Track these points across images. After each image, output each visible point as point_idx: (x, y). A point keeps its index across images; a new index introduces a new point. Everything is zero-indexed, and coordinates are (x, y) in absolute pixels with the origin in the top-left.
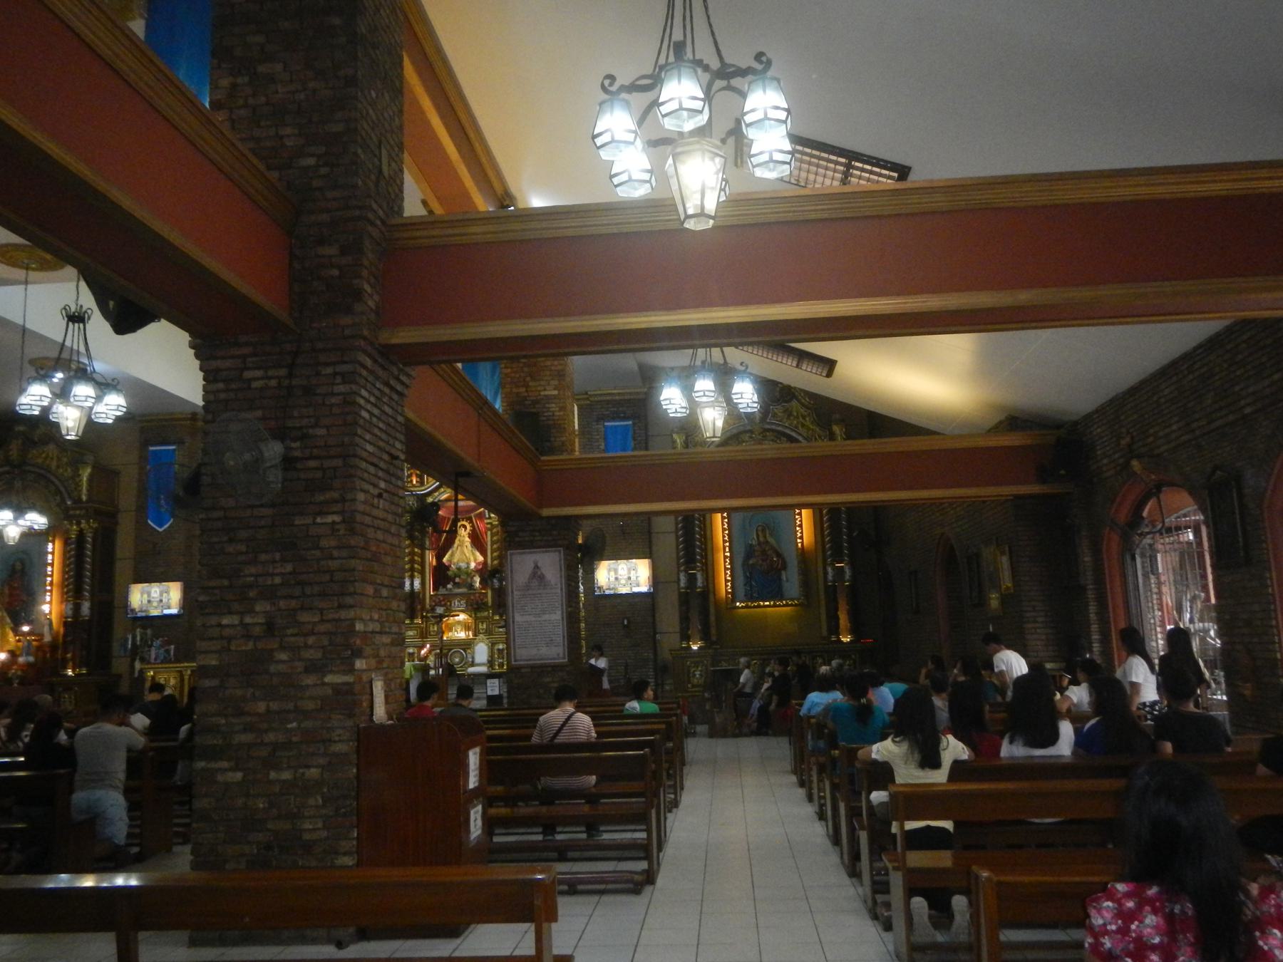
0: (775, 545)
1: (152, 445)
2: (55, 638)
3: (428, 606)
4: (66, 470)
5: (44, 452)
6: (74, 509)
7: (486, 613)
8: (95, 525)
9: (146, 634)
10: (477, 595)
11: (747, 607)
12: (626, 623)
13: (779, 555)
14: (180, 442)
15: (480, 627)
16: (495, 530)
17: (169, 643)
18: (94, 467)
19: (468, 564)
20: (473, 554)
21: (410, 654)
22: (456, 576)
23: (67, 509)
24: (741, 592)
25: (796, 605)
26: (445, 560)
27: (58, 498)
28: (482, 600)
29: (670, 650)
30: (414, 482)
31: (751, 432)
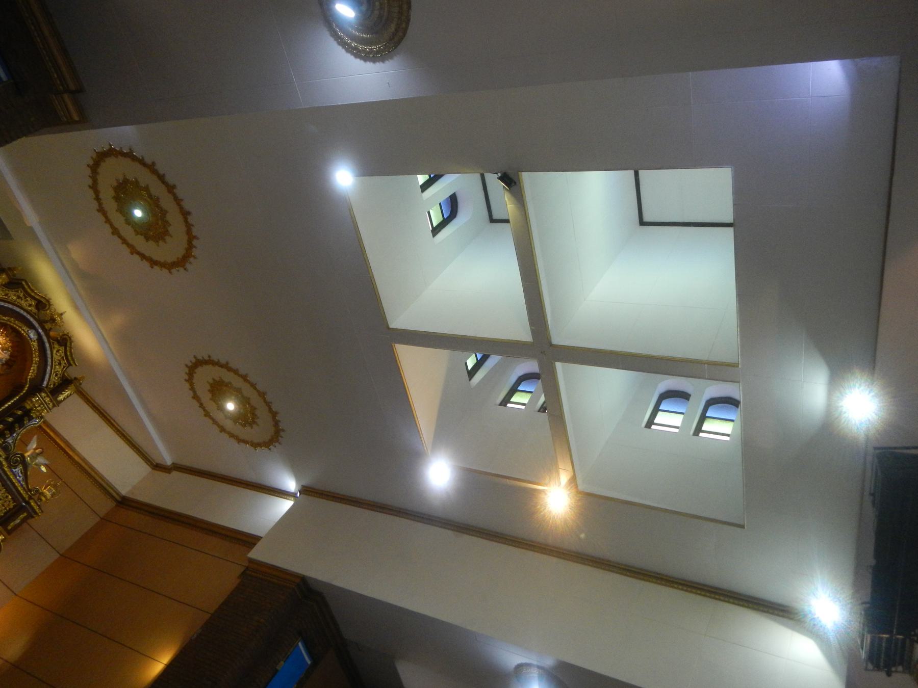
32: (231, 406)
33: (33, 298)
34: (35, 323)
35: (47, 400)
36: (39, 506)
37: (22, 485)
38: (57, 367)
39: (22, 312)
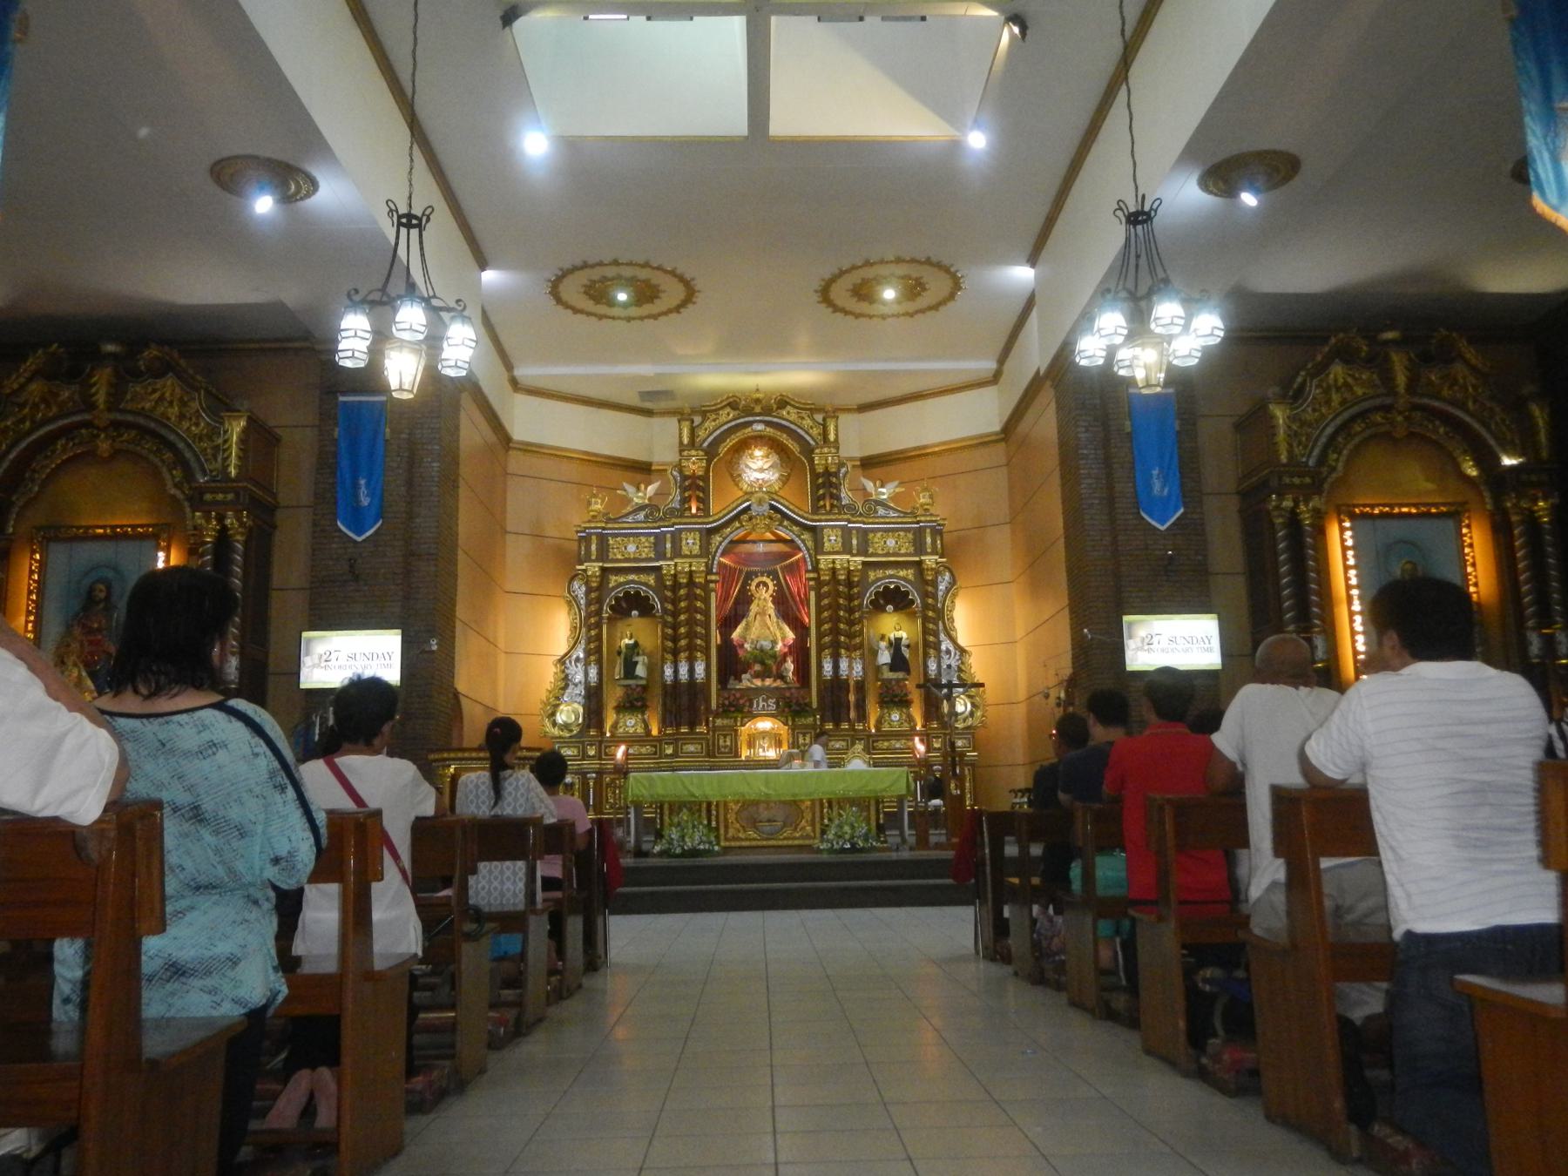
1: (344, 393)
3: (714, 705)
4: (197, 425)
5: (154, 391)
6: (214, 491)
7: (810, 720)
8: (250, 523)
10: (793, 691)
15: (801, 741)
16: (826, 589)
18: (251, 420)
19: (774, 642)
20: (781, 629)
22: (757, 660)
23: (201, 491)
26: (736, 635)
28: (804, 698)
30: (694, 511)
31: (1387, 409)
32: (889, 294)
33: (722, 408)
34: (746, 419)
35: (826, 450)
36: (931, 515)
37: (898, 517)
38: (804, 422)
39: (729, 425)
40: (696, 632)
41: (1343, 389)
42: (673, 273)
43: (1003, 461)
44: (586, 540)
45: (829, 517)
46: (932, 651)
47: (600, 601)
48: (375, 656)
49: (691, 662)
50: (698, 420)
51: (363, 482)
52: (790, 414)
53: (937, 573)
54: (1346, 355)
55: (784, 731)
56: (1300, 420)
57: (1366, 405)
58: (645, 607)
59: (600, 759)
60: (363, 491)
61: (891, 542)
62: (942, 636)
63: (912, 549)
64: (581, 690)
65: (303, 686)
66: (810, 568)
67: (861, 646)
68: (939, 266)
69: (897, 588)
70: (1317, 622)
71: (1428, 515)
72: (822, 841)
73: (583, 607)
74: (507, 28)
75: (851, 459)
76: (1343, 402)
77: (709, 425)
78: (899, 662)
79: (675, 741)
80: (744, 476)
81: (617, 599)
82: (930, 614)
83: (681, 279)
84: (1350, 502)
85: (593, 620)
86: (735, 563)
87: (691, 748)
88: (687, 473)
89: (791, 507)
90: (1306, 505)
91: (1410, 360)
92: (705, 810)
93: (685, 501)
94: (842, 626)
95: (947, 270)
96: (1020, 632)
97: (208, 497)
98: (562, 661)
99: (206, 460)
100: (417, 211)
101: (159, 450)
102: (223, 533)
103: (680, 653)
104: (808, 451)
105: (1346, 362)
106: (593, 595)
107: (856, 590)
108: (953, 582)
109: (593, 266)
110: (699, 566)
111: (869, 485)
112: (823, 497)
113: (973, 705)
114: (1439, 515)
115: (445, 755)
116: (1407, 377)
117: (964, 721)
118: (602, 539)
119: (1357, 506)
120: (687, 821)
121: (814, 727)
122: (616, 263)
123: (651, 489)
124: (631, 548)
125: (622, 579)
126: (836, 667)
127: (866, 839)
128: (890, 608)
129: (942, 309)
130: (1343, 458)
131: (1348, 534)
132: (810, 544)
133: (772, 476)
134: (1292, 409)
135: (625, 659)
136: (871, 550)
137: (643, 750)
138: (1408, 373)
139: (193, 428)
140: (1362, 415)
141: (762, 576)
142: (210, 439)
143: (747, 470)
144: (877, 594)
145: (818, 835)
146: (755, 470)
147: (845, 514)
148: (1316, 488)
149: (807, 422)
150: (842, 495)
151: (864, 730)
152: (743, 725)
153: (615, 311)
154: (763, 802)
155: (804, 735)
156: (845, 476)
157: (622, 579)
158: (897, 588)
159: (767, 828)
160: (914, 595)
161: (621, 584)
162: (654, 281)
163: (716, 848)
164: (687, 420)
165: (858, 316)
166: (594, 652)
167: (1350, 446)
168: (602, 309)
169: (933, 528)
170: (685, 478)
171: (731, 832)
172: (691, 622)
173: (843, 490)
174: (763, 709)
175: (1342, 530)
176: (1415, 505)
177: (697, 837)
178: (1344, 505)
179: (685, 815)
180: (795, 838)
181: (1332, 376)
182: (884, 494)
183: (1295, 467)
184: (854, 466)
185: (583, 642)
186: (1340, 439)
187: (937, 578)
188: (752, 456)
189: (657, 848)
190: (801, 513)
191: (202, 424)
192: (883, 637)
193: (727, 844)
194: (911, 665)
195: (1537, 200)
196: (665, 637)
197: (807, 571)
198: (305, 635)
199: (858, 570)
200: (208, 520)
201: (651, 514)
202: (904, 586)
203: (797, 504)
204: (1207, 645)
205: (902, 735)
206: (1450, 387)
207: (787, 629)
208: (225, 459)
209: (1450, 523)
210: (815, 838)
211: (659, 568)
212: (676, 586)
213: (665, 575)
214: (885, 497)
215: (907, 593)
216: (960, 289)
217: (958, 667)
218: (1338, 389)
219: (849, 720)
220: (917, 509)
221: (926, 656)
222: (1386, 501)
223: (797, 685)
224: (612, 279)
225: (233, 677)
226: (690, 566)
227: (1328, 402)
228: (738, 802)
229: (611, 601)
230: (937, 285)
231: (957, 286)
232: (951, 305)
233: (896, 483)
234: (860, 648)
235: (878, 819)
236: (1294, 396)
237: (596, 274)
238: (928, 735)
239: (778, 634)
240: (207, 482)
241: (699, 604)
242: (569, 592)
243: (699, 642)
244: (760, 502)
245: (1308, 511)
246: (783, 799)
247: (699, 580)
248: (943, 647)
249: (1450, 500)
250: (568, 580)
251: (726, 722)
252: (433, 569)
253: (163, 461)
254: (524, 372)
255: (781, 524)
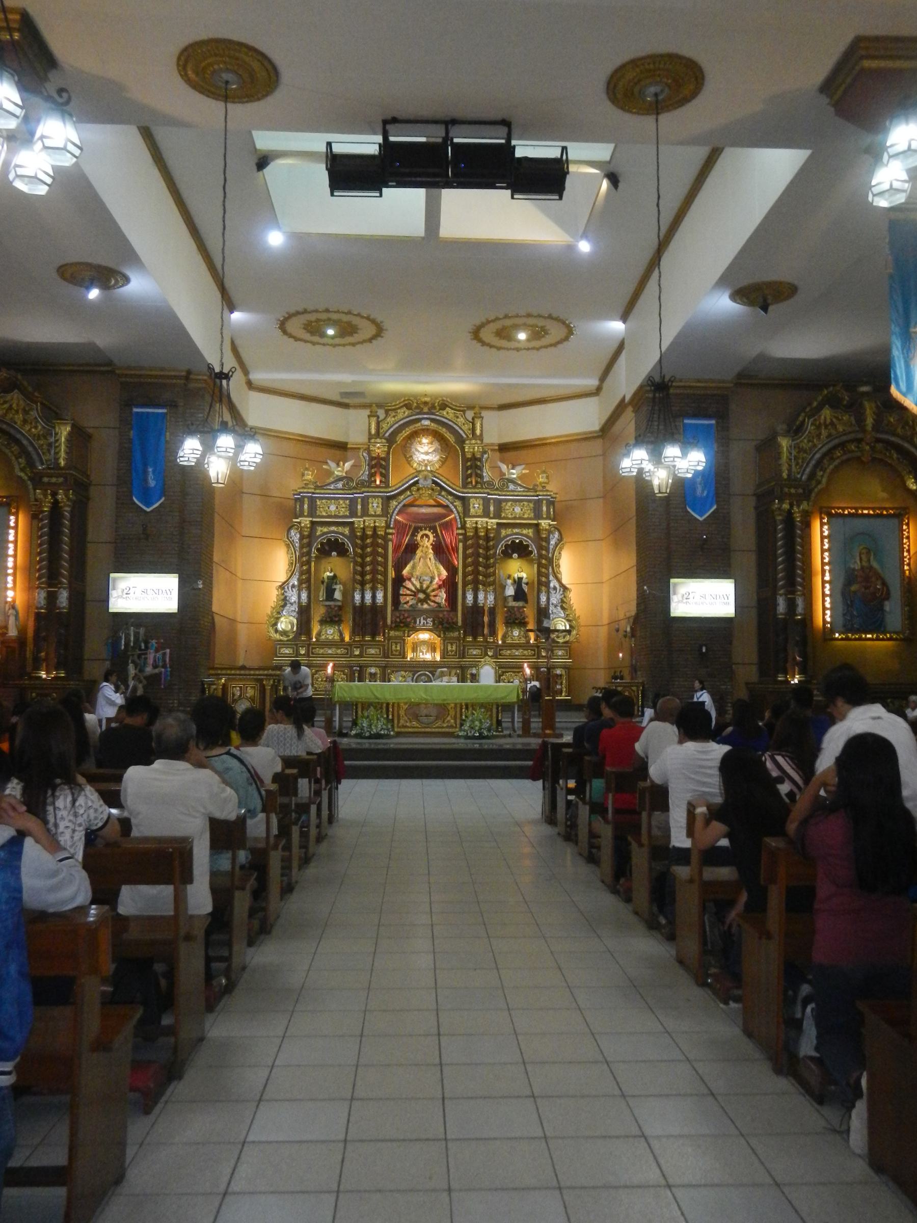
0: (880, 571)
1: (138, 406)
2: (22, 631)
4: (36, 427)
5: (5, 402)
6: (50, 476)
9: (138, 633)
10: (445, 613)
11: (847, 639)
12: (704, 650)
13: (884, 584)
14: (172, 405)
15: (449, 648)
16: (470, 542)
17: (164, 649)
18: (74, 426)
20: (437, 568)
21: (371, 674)
23: (41, 475)
24: (840, 621)
25: (901, 640)
27: (22, 461)
28: (452, 619)
29: (747, 684)
30: (378, 482)
31: (859, 441)
32: (522, 336)
33: (402, 407)
34: (417, 417)
35: (473, 441)
37: (523, 491)
38: (459, 420)
40: (377, 570)
41: (830, 427)
42: (368, 318)
43: (600, 452)
44: (301, 501)
45: (474, 491)
46: (543, 588)
47: (309, 545)
48: (160, 592)
49: (374, 591)
50: (382, 416)
51: (150, 470)
52: (448, 413)
53: (550, 532)
54: (834, 402)
55: (437, 640)
56: (799, 448)
57: (844, 438)
58: (342, 551)
59: (309, 656)
60: (151, 476)
61: (518, 510)
62: (551, 578)
63: (532, 515)
64: (295, 607)
65: (111, 611)
66: (460, 526)
67: (493, 583)
68: (557, 319)
69: (521, 542)
70: (799, 588)
71: (881, 516)
72: (461, 730)
73: (298, 549)
74: (260, 173)
75: (492, 445)
76: (830, 435)
77: (390, 420)
78: (520, 595)
79: (361, 646)
80: (414, 457)
81: (322, 544)
82: (544, 561)
83: (373, 321)
84: (830, 505)
85: (304, 559)
86: (408, 520)
87: (372, 651)
88: (374, 455)
89: (448, 482)
90: (798, 506)
91: (877, 407)
92: (385, 708)
93: (372, 475)
94: (481, 569)
95: (564, 323)
96: (606, 577)
97: (46, 480)
98: (282, 587)
99: (44, 453)
100: (225, 371)
101: (8, 444)
102: (55, 505)
103: (366, 584)
104: (461, 441)
105: (832, 407)
106: (305, 541)
107: (491, 543)
108: (560, 540)
109: (309, 313)
110: (380, 523)
111: (504, 467)
112: (470, 476)
113: (570, 626)
114: (889, 516)
115: (219, 672)
116: (874, 419)
117: (564, 637)
118: (312, 501)
119: (834, 508)
120: (373, 715)
121: (458, 639)
122: (327, 311)
123: (348, 465)
124: (333, 508)
125: (325, 530)
126: (476, 597)
127: (489, 730)
128: (515, 555)
129: (560, 346)
130: (826, 475)
131: (826, 527)
132: (460, 509)
133: (434, 458)
134: (793, 441)
135: (327, 588)
136: (503, 515)
137: (339, 651)
138: (875, 417)
139: (33, 430)
140: (842, 445)
141: (425, 530)
142: (45, 437)
143: (416, 453)
144: (506, 546)
145: (458, 726)
146: (422, 453)
147: (486, 488)
148: (806, 496)
149: (461, 420)
150: (484, 474)
151: (494, 642)
152: (409, 636)
153: (324, 340)
154: (424, 703)
155: (452, 645)
156: (487, 460)
157: (325, 530)
158: (521, 542)
159: (424, 719)
160: (533, 548)
161: (324, 534)
162: (354, 323)
163: (392, 733)
164: (374, 416)
165: (499, 348)
166: (306, 581)
167: (831, 467)
168: (316, 339)
169: (547, 500)
170: (372, 459)
171: (402, 722)
172: (374, 563)
173: (485, 470)
174: (424, 625)
175: (822, 524)
176: (873, 509)
177: (379, 726)
178: (825, 507)
179: (372, 711)
180: (443, 727)
181: (823, 417)
182: (514, 474)
183: (792, 481)
184: (492, 450)
185: (297, 574)
186: (825, 461)
187: (549, 536)
188: (420, 443)
189: (353, 732)
190: (454, 487)
191: (40, 427)
192: (509, 577)
193: (399, 730)
194: (529, 597)
195: (894, 391)
196: (355, 572)
197: (458, 528)
198: (112, 575)
199: (493, 529)
200: (45, 496)
201: (347, 484)
202: (526, 541)
203: (453, 480)
204: (726, 600)
205: (520, 646)
206: (903, 427)
207: (442, 568)
208: (56, 453)
209: (896, 521)
210: (456, 727)
211: (353, 523)
212: (364, 537)
213: (357, 528)
214: (515, 476)
215: (528, 546)
216: (572, 334)
217: (562, 599)
218: (826, 427)
219: (483, 635)
220: (537, 485)
221: (539, 592)
222: (853, 505)
223: (448, 609)
224: (324, 321)
225: (64, 605)
226: (375, 522)
227: (819, 436)
228: (406, 704)
229: (317, 545)
230: (556, 332)
231: (570, 332)
232: (565, 343)
233: (523, 466)
234: (492, 585)
235: (497, 717)
236: (795, 431)
237: (313, 317)
238: (538, 647)
239: (436, 573)
240: (44, 469)
241: (380, 550)
242: (288, 538)
243: (379, 577)
244: (425, 478)
245: (799, 512)
246: (436, 702)
247: (381, 533)
248: (552, 585)
249: (896, 505)
250: (287, 529)
251: (397, 633)
252: (199, 531)
253: (12, 452)
254: (257, 376)
255: (439, 495)
